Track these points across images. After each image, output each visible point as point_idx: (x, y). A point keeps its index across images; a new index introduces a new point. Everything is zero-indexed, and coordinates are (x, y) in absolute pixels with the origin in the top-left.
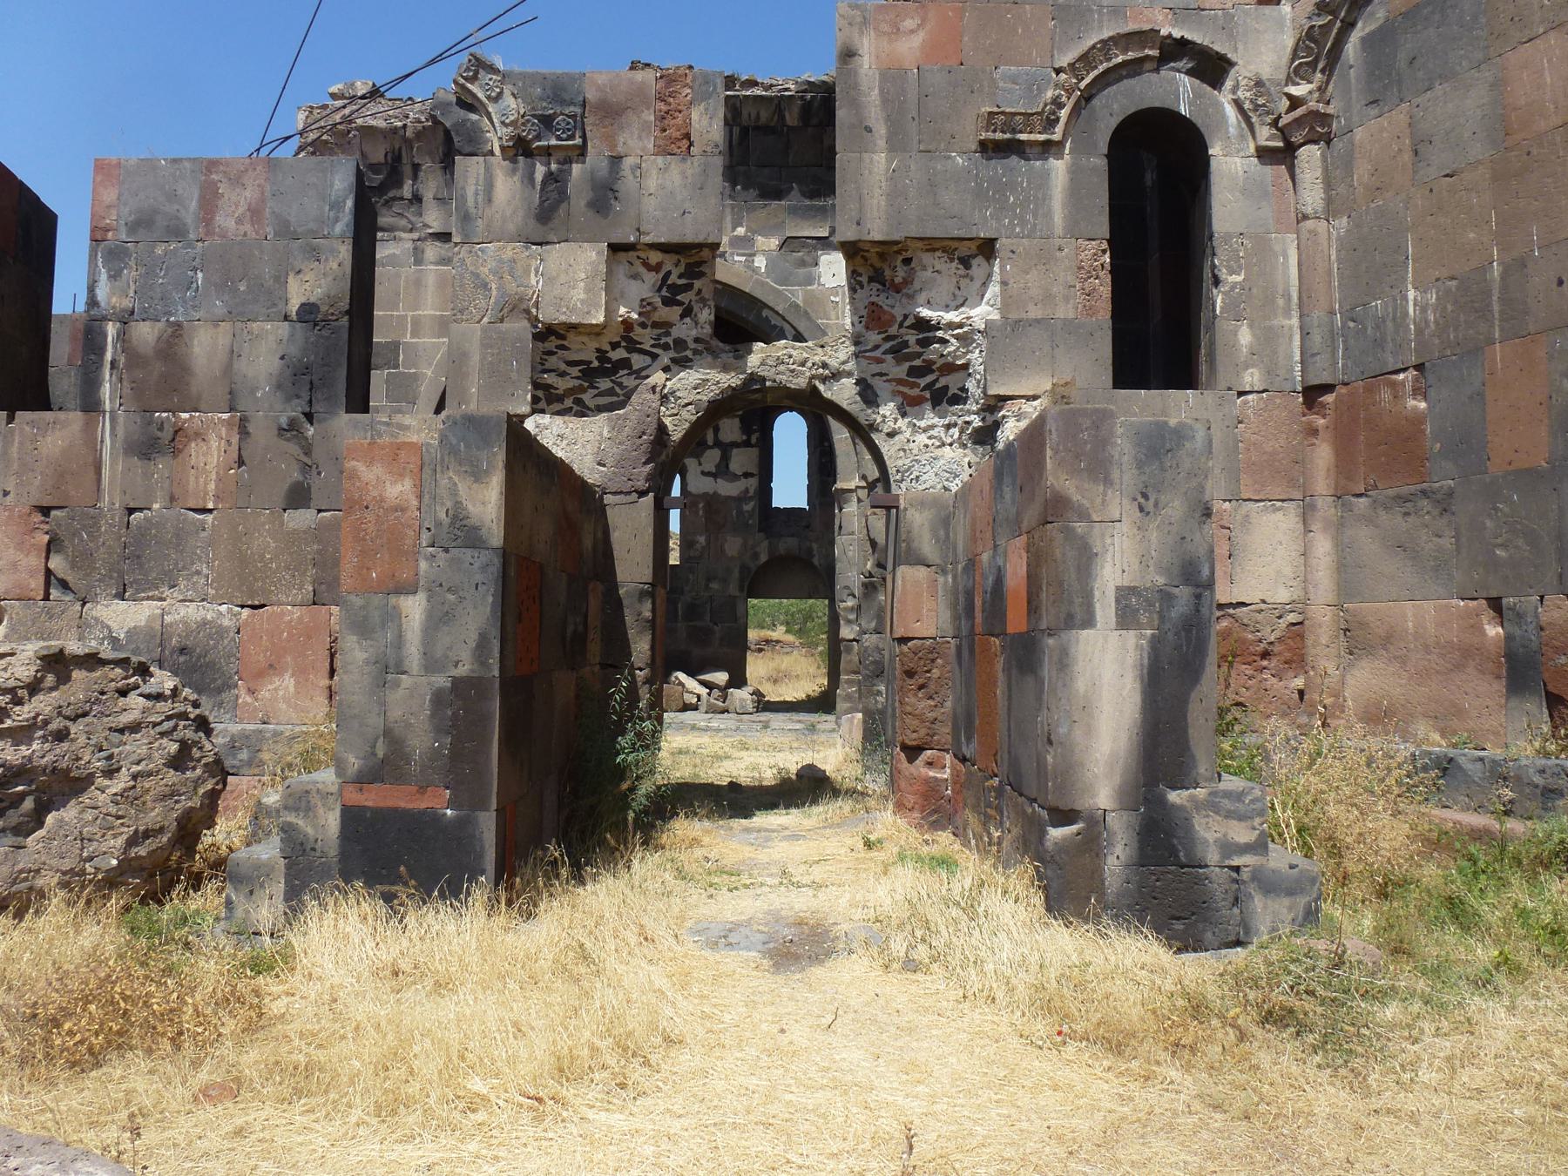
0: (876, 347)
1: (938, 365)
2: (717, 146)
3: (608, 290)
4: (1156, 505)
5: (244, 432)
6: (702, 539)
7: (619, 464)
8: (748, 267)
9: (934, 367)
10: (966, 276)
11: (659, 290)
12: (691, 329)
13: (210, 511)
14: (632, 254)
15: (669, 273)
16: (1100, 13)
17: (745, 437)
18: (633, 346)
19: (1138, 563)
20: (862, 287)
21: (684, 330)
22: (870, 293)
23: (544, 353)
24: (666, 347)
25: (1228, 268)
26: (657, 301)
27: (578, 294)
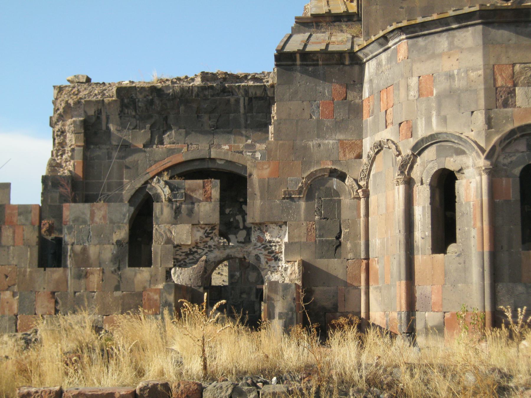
0: (260, 247)
3: (191, 236)
5: (103, 272)
6: (238, 274)
7: (194, 279)
11: (205, 234)
13: (95, 292)
14: (198, 226)
15: (206, 230)
18: (198, 247)
20: (256, 231)
21: (211, 243)
24: (206, 247)
25: (345, 228)
26: (204, 237)
27: (184, 237)
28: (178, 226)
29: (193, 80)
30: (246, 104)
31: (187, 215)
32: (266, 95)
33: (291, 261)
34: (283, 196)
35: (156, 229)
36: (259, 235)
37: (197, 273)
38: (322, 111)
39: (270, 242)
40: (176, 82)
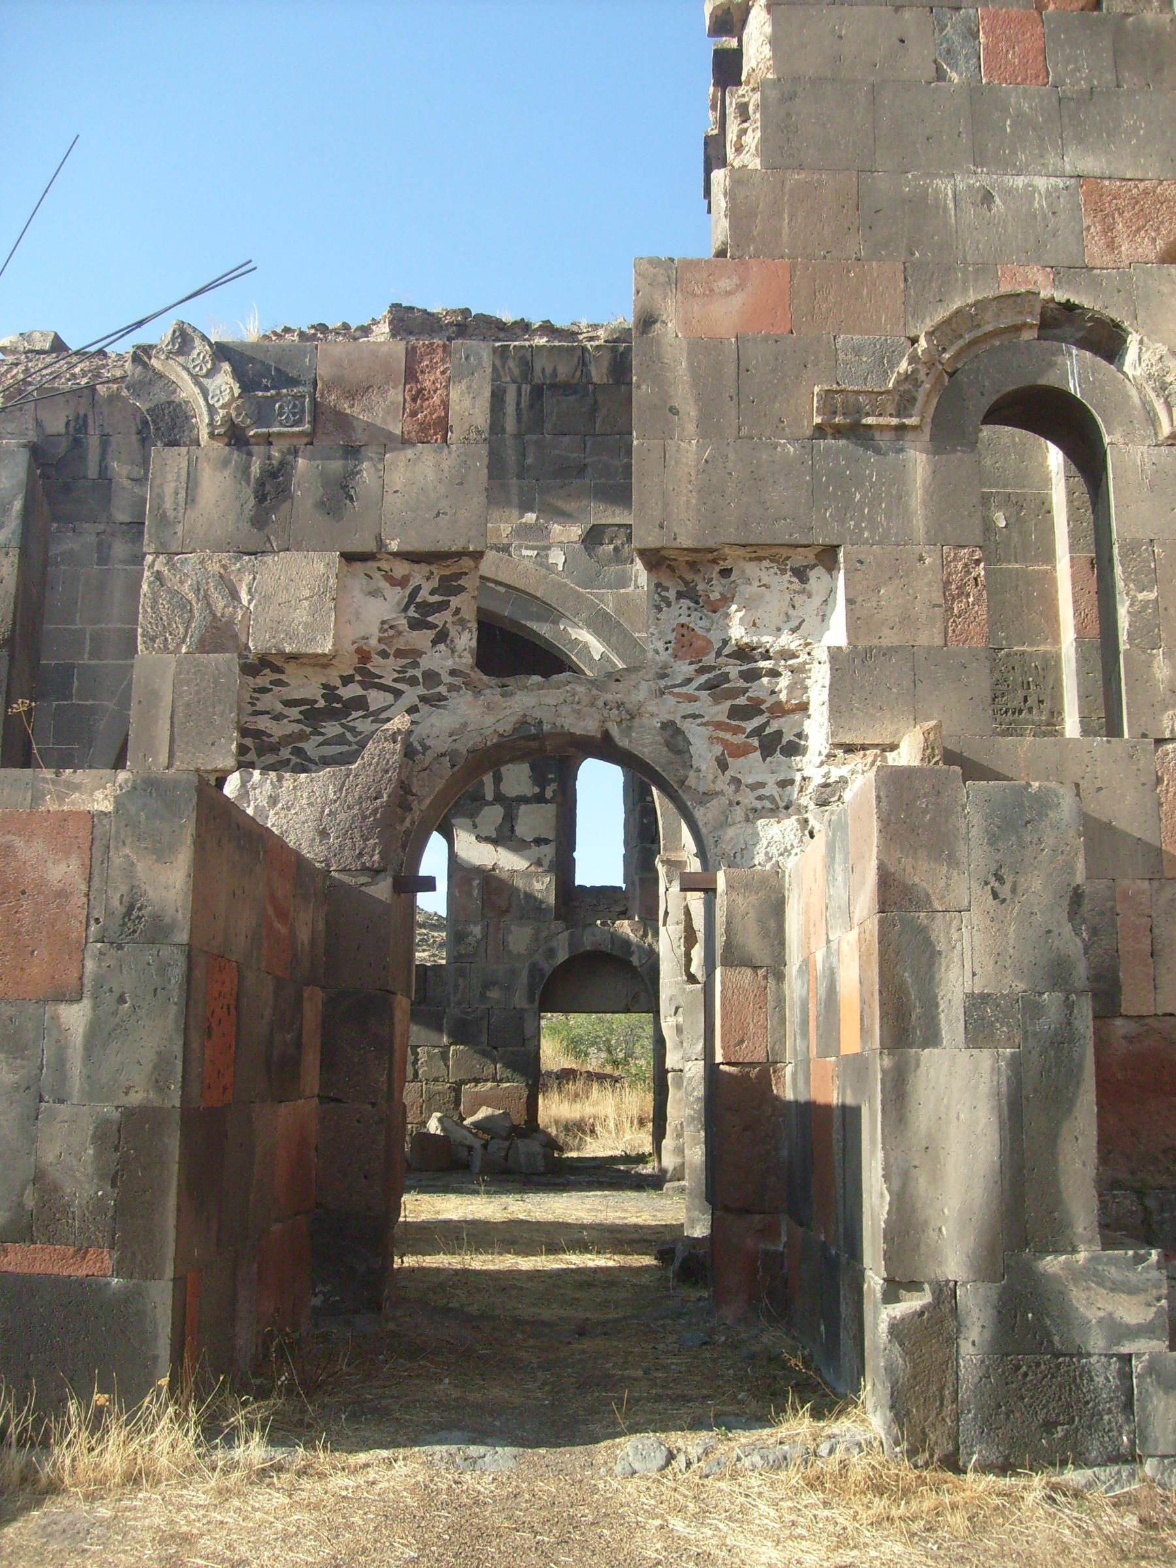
0: (689, 681)
1: (767, 705)
2: (479, 433)
4: (1014, 890)
6: (477, 930)
8: (541, 565)
9: (763, 707)
10: (803, 591)
11: (406, 609)
12: (446, 659)
15: (418, 588)
16: (965, 271)
17: (537, 790)
18: (370, 680)
19: (992, 962)
20: (669, 605)
21: (437, 660)
22: (679, 613)
23: (255, 690)
24: (413, 681)
26: (403, 623)
27: (301, 616)
28: (269, 559)
29: (365, 330)
30: (523, 405)
31: (321, 505)
32: (584, 380)
33: (864, 747)
34: (818, 420)
35: (158, 576)
36: (684, 620)
37: (360, 801)
38: (992, 53)
39: (744, 653)
40: (314, 335)
